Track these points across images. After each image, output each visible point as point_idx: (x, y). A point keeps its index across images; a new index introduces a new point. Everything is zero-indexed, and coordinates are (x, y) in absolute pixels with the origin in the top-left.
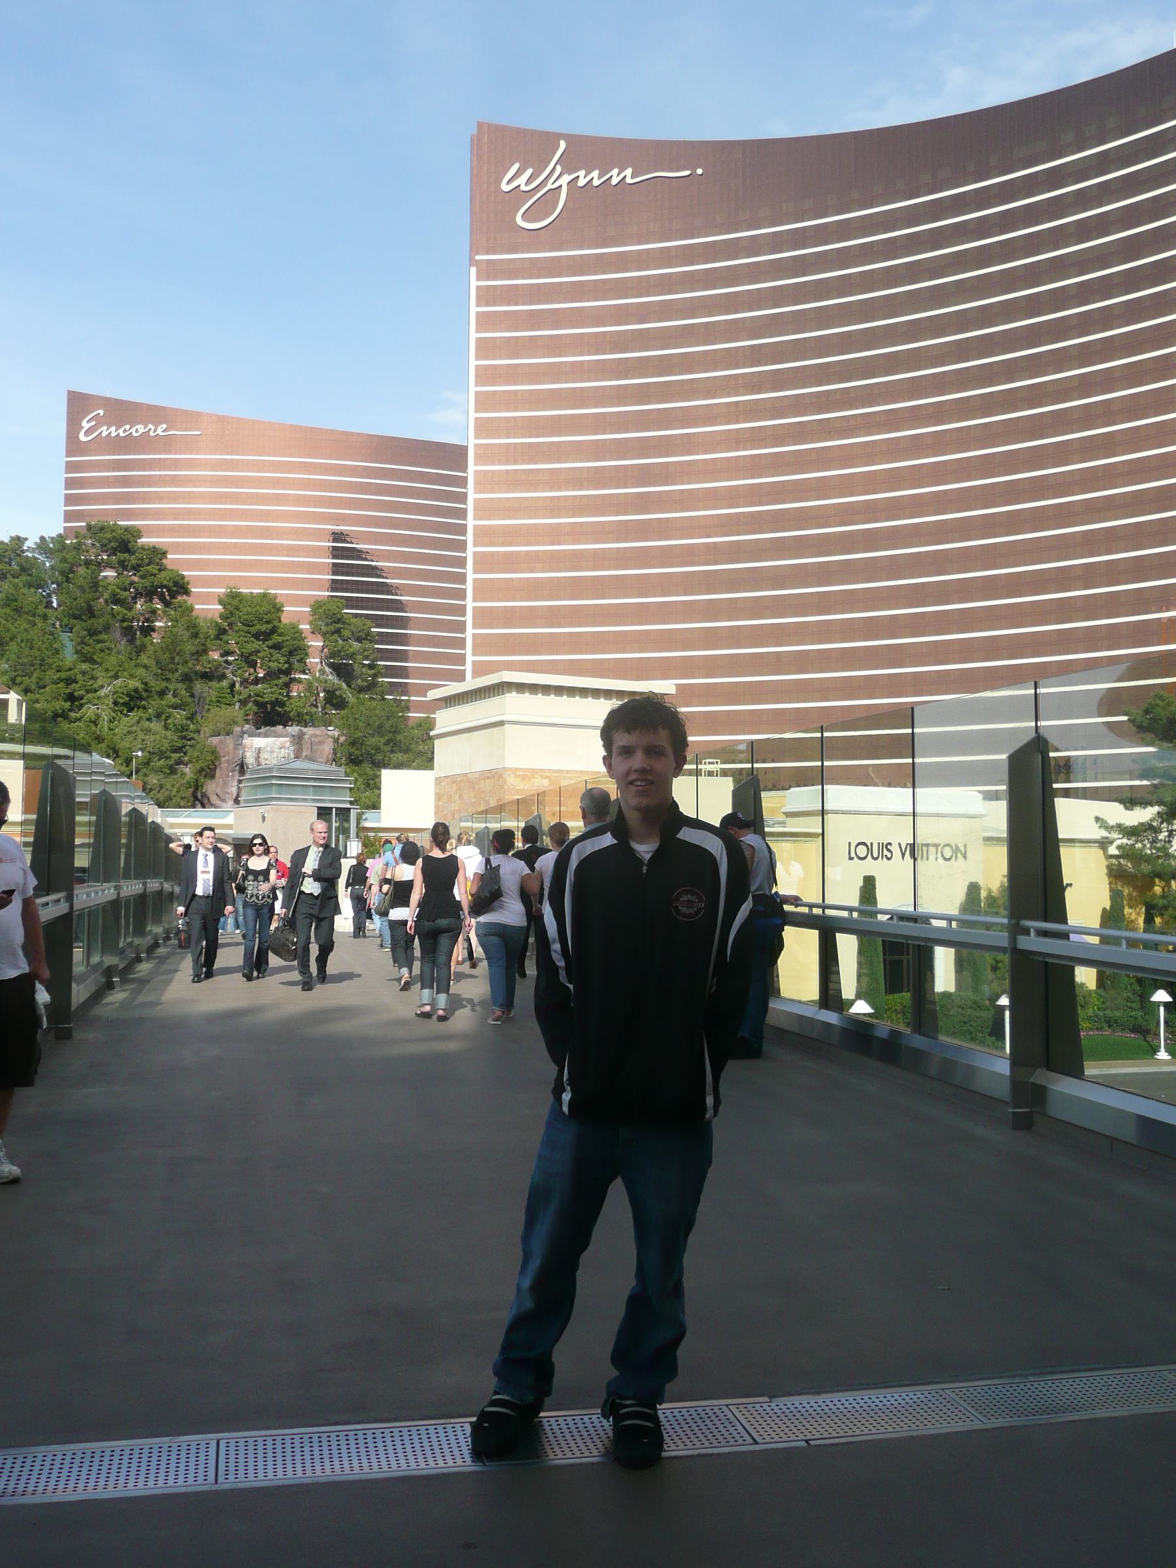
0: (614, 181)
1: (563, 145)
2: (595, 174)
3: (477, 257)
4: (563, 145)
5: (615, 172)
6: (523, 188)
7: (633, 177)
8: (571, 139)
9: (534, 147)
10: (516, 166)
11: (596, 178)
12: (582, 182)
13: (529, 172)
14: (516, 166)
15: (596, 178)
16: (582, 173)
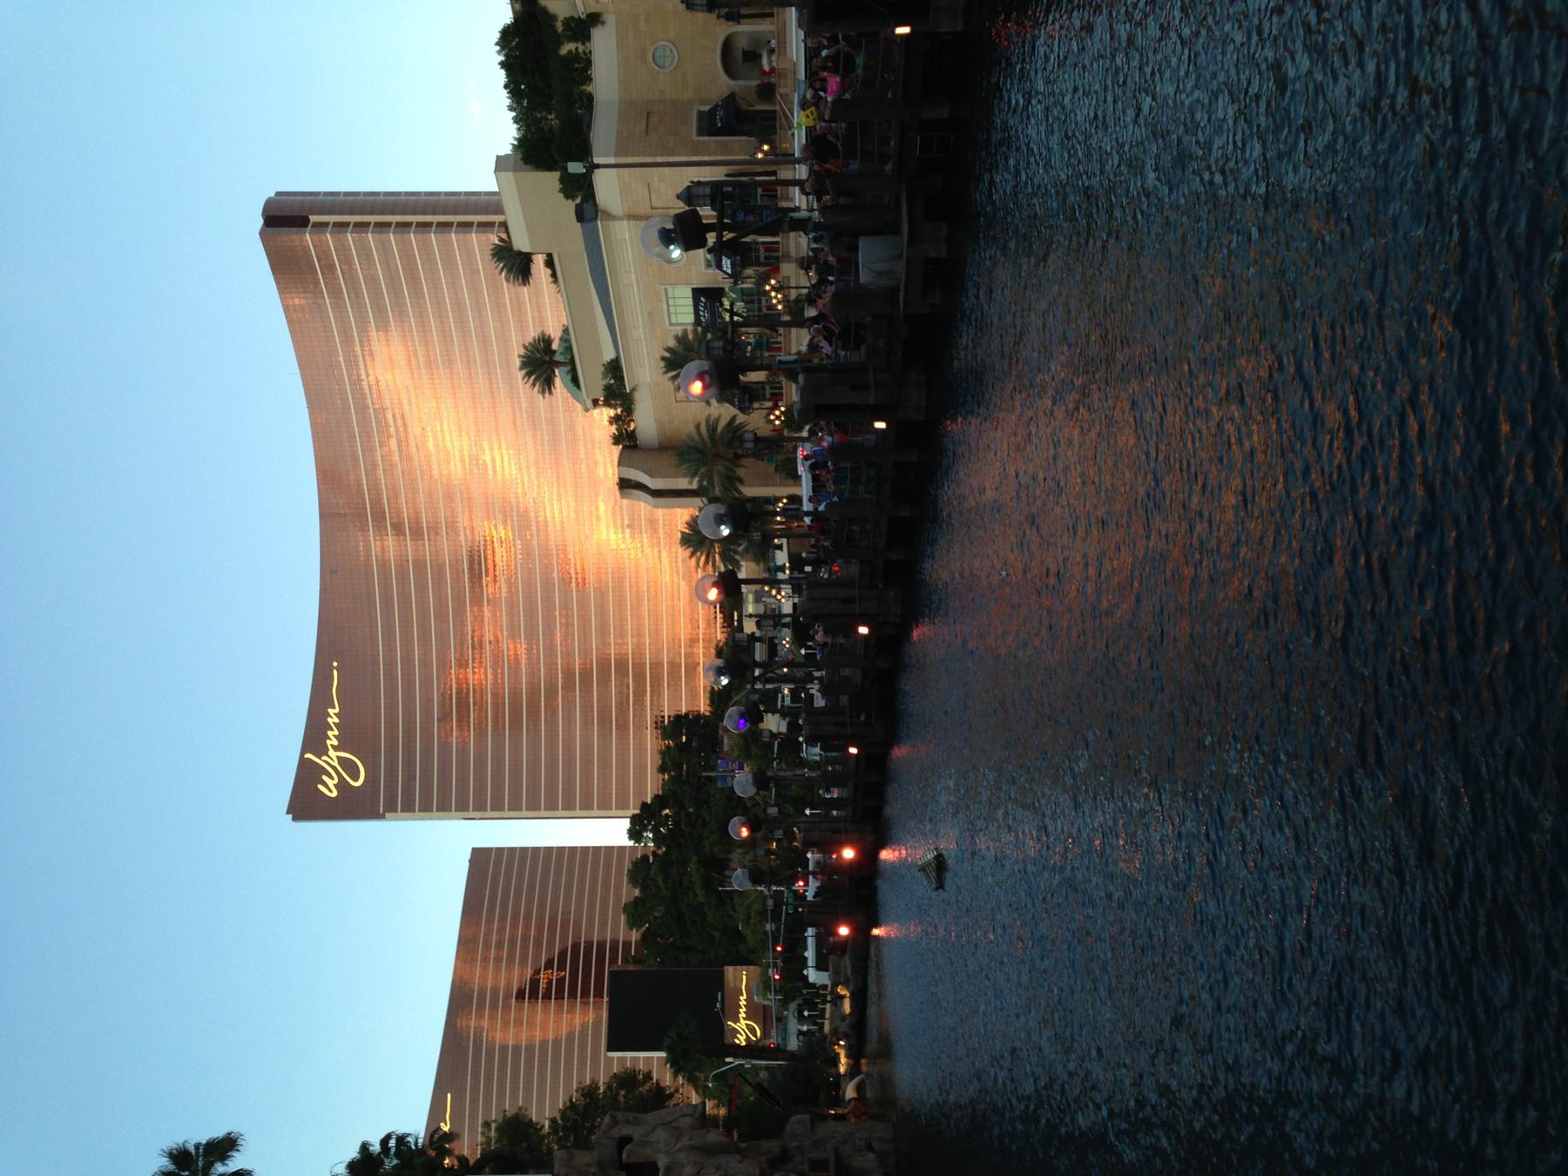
1: (308, 756)
2: (330, 733)
4: (308, 756)
8: (303, 752)
9: (307, 775)
10: (320, 787)
12: (335, 743)
13: (325, 778)
14: (320, 787)
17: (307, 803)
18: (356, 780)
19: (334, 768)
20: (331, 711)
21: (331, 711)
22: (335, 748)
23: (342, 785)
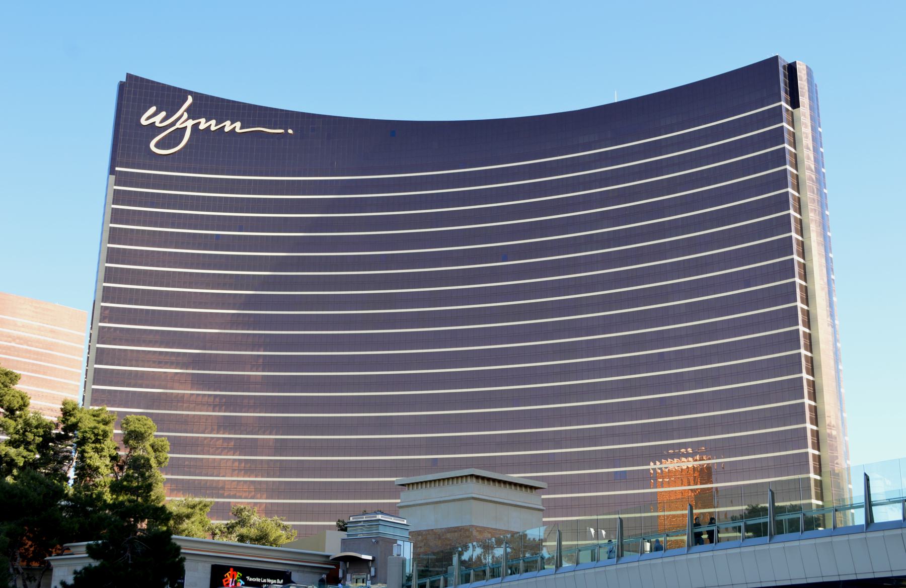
0: (227, 129)
1: (190, 99)
2: (213, 122)
3: (117, 169)
4: (190, 99)
5: (228, 123)
6: (157, 124)
7: (241, 128)
8: (197, 96)
9: (169, 97)
10: (153, 109)
11: (213, 125)
13: (163, 114)
15: (213, 125)
16: (203, 120)
17: (136, 94)
18: (157, 145)
19: (174, 124)
20: (238, 125)
21: (238, 125)
22: (195, 127)
23: (153, 130)
